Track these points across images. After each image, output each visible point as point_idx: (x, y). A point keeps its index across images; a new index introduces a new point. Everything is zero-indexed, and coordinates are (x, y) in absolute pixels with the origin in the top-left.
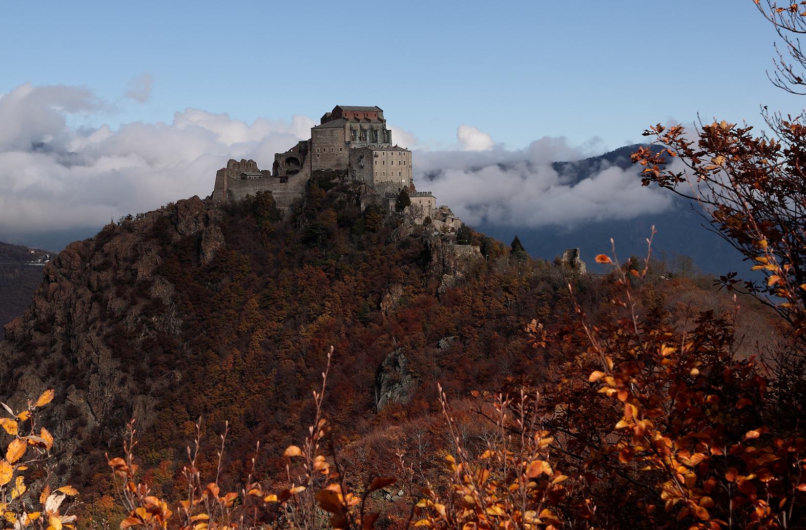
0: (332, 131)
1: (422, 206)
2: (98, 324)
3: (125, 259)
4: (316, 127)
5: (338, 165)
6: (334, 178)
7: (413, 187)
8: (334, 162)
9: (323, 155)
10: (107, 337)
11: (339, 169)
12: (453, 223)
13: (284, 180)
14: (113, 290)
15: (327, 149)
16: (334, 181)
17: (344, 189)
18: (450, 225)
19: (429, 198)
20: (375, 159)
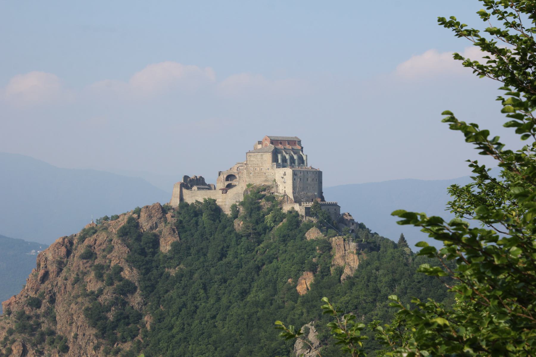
0: (262, 155)
1: (330, 213)
2: (80, 300)
3: (104, 250)
4: (250, 152)
5: (266, 181)
6: (265, 190)
7: (323, 199)
8: (263, 179)
9: (255, 173)
10: (87, 309)
11: (266, 184)
12: (353, 226)
13: (225, 191)
14: (93, 275)
15: (258, 169)
16: (263, 193)
17: (271, 198)
18: (351, 228)
19: (335, 207)
20: (295, 177)
